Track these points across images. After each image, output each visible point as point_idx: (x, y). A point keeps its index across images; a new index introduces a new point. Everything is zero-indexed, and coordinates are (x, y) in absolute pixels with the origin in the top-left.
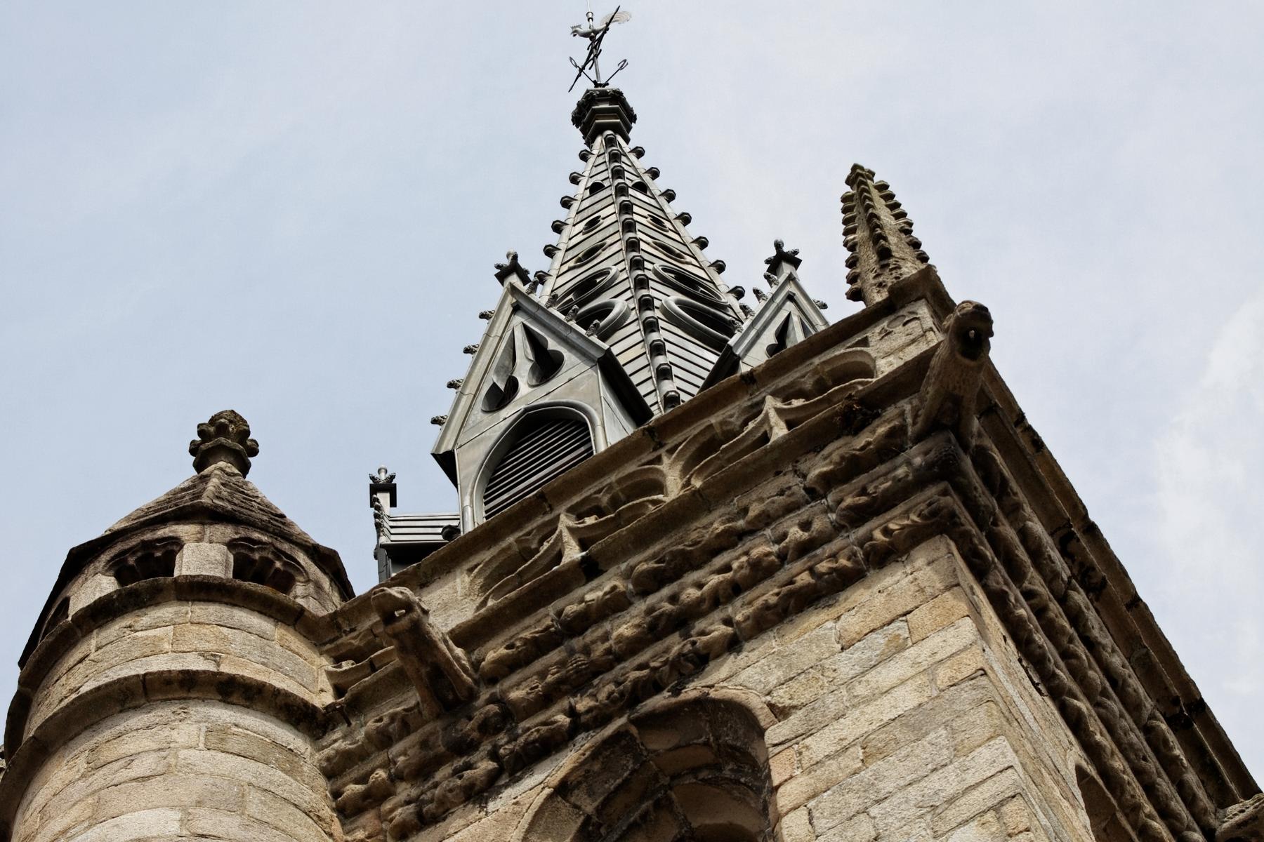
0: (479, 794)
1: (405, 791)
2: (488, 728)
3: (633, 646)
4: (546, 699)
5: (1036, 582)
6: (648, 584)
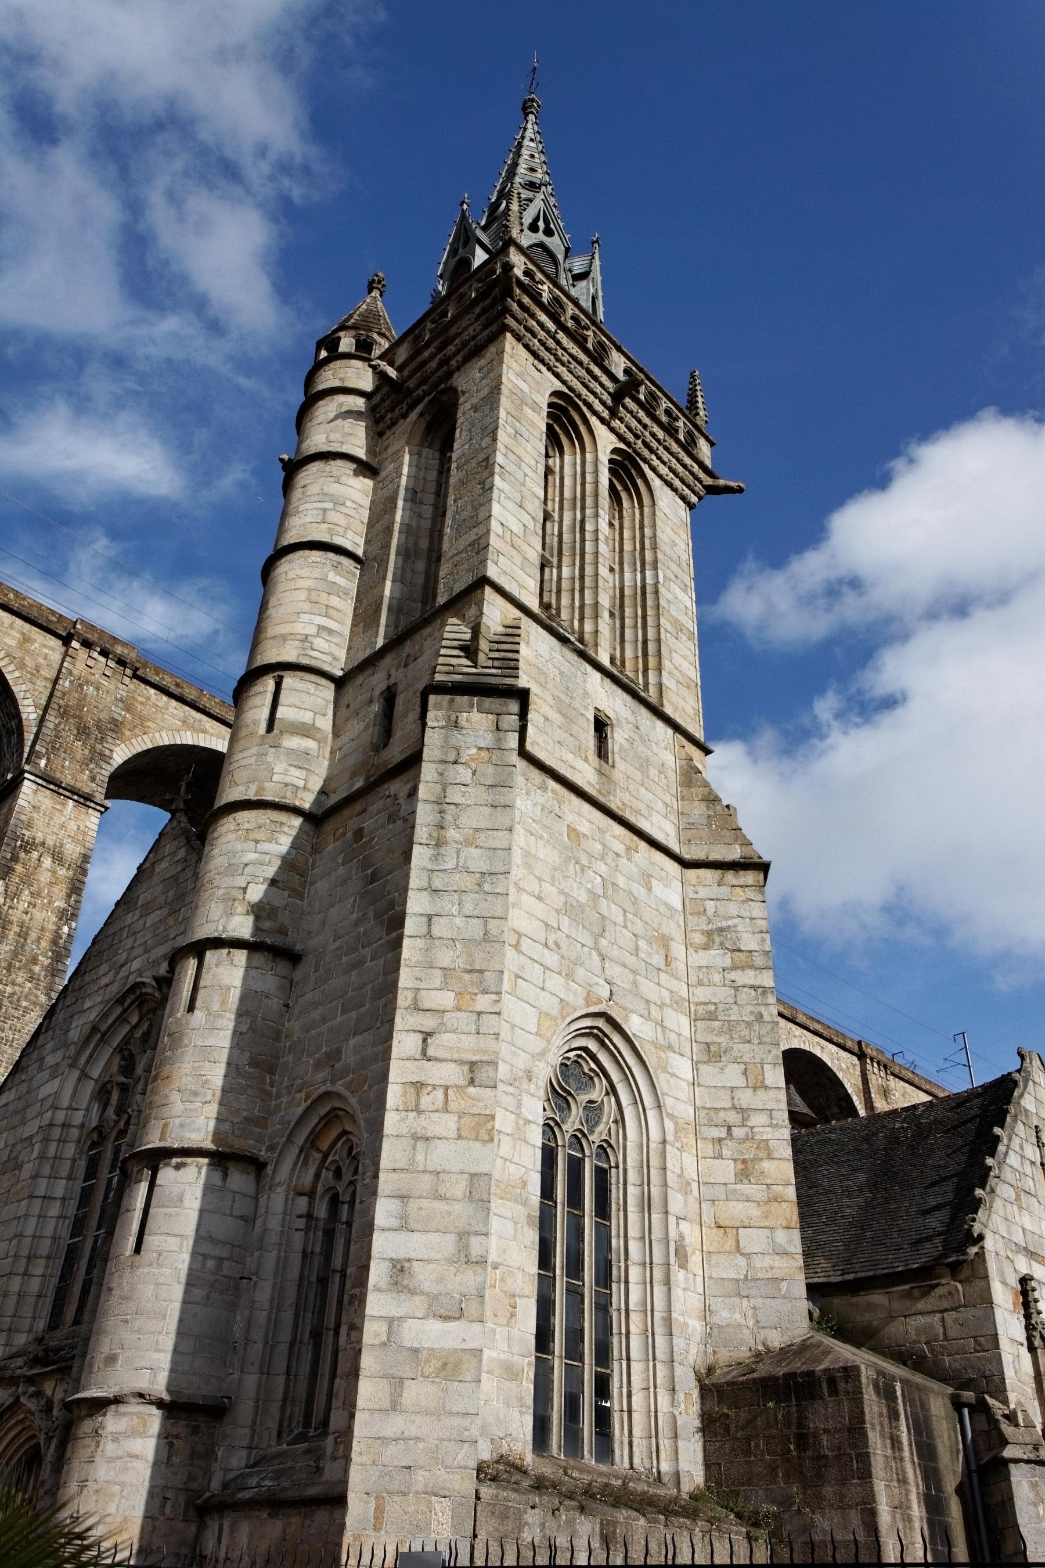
0: (404, 416)
1: (389, 416)
3: (437, 369)
5: (542, 334)
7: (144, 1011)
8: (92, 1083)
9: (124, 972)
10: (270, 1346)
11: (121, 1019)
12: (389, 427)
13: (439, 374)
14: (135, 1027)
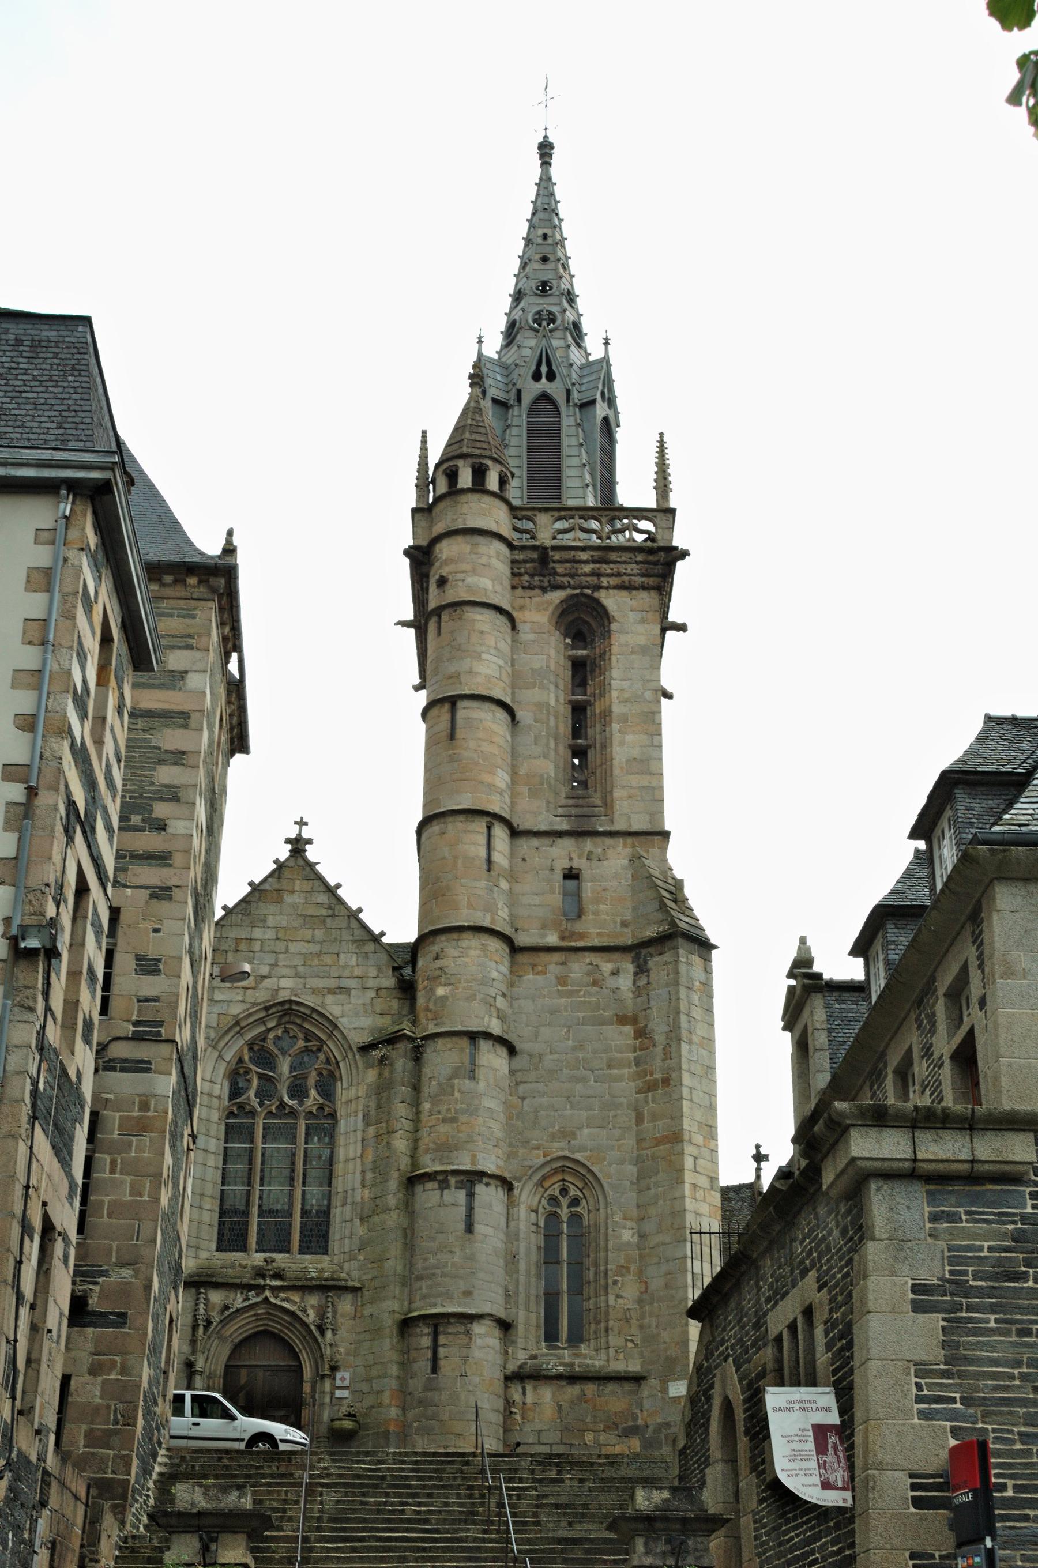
0: (544, 590)
1: (526, 578)
2: (550, 575)
3: (586, 575)
4: (565, 575)
6: (594, 562)
7: (283, 1021)
8: (224, 1064)
9: (267, 983)
10: (528, 1297)
11: (262, 1021)
12: (523, 588)
13: (588, 579)
14: (269, 1030)
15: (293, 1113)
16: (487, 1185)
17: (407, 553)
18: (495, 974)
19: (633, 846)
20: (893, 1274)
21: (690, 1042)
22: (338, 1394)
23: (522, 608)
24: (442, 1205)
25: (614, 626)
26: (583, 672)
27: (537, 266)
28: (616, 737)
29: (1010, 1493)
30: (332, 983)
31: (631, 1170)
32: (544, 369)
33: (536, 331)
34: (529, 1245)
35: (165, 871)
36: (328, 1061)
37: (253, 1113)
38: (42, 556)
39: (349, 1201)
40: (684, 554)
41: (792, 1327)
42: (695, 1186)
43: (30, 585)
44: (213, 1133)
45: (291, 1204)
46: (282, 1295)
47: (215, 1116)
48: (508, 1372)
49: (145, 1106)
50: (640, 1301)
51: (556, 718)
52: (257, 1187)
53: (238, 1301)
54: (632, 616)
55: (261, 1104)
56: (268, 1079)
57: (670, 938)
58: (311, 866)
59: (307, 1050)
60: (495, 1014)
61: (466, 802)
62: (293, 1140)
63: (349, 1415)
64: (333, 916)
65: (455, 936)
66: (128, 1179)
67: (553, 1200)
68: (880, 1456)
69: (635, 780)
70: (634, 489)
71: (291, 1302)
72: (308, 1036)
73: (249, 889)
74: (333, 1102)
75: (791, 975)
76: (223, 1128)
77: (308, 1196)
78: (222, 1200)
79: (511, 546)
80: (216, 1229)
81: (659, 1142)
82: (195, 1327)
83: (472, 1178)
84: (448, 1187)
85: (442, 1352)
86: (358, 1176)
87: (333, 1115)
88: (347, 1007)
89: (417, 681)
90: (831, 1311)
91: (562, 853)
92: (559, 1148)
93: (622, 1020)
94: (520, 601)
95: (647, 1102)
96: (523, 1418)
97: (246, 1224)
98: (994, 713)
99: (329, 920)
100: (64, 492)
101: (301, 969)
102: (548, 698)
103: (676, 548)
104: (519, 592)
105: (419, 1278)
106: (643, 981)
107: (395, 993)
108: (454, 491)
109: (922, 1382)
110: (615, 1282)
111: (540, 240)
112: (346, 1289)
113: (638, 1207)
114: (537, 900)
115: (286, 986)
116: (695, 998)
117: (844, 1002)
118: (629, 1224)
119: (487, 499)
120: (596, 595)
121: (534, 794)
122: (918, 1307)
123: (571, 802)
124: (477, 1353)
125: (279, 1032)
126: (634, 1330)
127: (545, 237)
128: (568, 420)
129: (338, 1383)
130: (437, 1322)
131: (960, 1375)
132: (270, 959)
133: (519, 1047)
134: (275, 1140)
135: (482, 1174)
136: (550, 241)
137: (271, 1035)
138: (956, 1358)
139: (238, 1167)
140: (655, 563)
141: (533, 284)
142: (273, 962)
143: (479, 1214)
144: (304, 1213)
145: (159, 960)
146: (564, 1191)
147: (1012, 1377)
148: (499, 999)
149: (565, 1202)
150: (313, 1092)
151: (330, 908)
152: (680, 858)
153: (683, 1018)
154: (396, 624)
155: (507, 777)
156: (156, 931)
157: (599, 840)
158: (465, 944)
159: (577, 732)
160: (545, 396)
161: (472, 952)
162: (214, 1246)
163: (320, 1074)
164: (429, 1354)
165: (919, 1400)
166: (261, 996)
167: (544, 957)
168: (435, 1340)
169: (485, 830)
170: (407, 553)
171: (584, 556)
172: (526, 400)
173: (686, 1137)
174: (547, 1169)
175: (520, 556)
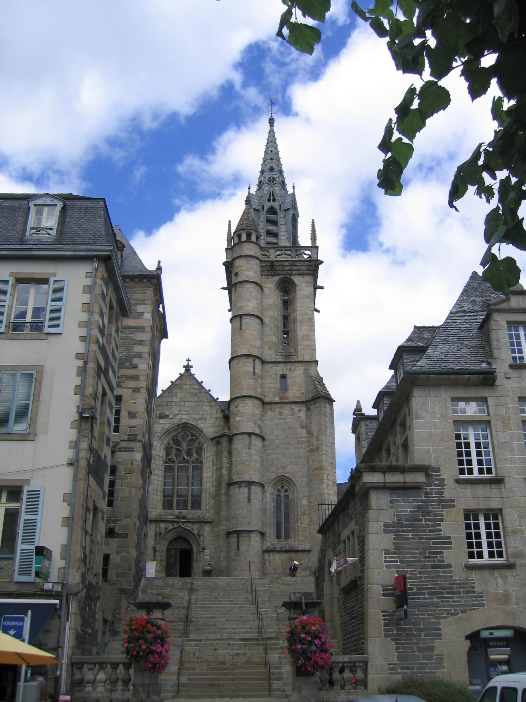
0: (272, 276)
1: (266, 272)
3: (287, 270)
6: (290, 266)
8: (164, 445)
9: (178, 417)
14: (179, 433)
15: (188, 462)
16: (255, 486)
17: (224, 264)
18: (257, 412)
19: (305, 366)
20: (377, 521)
21: (326, 435)
22: (206, 557)
23: (265, 282)
24: (240, 493)
25: (297, 288)
26: (287, 304)
27: (269, 161)
28: (299, 328)
29: (415, 591)
30: (200, 416)
31: (305, 479)
32: (272, 198)
33: (269, 184)
34: (270, 506)
35: (137, 382)
36: (199, 444)
37: (174, 462)
38: (88, 282)
39: (208, 492)
40: (322, 262)
41: (348, 538)
42: (327, 485)
43: (84, 292)
44: (160, 469)
45: (188, 493)
46: (186, 524)
47: (161, 463)
48: (264, 549)
49: (132, 464)
50: (309, 525)
51: (278, 321)
52: (176, 488)
53: (170, 527)
54: (304, 284)
55: (177, 459)
56: (179, 450)
57: (319, 398)
58: (193, 375)
59: (192, 440)
60: (257, 426)
61: (245, 352)
62: (188, 471)
63: (209, 564)
64: (200, 393)
65: (243, 399)
66: (127, 488)
67: (279, 490)
68: (372, 581)
69: (306, 343)
70: (304, 240)
71: (189, 527)
72: (192, 435)
73: (171, 384)
74: (202, 458)
75: (354, 414)
76: (164, 467)
77: (194, 490)
78: (164, 492)
79: (261, 261)
80: (162, 502)
81: (315, 469)
82: (156, 535)
83: (249, 484)
84: (242, 487)
85: (240, 543)
86: (211, 483)
87: (201, 462)
88: (206, 425)
89: (229, 308)
90: (359, 533)
91: (280, 369)
92: (280, 472)
93: (302, 427)
94: (264, 280)
95: (311, 456)
96: (269, 565)
97: (172, 500)
98: (417, 325)
99: (199, 394)
100: (95, 259)
101: (189, 411)
102: (273, 314)
103: (319, 260)
104: (264, 277)
105: (232, 518)
106: (309, 414)
107: (223, 419)
108: (240, 242)
109: (387, 556)
110: (301, 518)
111: (270, 152)
112: (207, 522)
113: (308, 492)
114: (272, 386)
115: (184, 418)
116: (327, 419)
117: (372, 423)
118: (305, 498)
119: (252, 244)
120: (291, 277)
121: (270, 348)
122: (386, 532)
123: (283, 351)
124: (253, 544)
125: (182, 434)
126: (307, 534)
127: (272, 151)
128: (281, 215)
129: (205, 554)
130: (239, 533)
131: (399, 553)
132: (178, 408)
133: (266, 437)
134: (182, 471)
135: (253, 482)
136: (273, 152)
137: (179, 435)
138: (398, 548)
139: (169, 480)
140: (312, 266)
141: (268, 167)
142: (179, 409)
143: (253, 496)
144: (193, 496)
145: (136, 413)
146: (282, 487)
147: (416, 553)
148: (259, 421)
149: (282, 491)
150: (195, 454)
151: (199, 390)
152: (322, 370)
153: (323, 426)
154: (222, 288)
155: (260, 343)
156: (135, 403)
157: (293, 364)
158: (246, 402)
159: (285, 326)
160: (272, 207)
161: (249, 405)
162: (161, 508)
163: (197, 448)
164: (236, 544)
165: (386, 562)
166: (176, 421)
167: (274, 406)
168: (238, 539)
169: (253, 361)
170: (224, 264)
171: (286, 264)
172: (266, 209)
173: (324, 467)
174: (276, 480)
175: (263, 264)
